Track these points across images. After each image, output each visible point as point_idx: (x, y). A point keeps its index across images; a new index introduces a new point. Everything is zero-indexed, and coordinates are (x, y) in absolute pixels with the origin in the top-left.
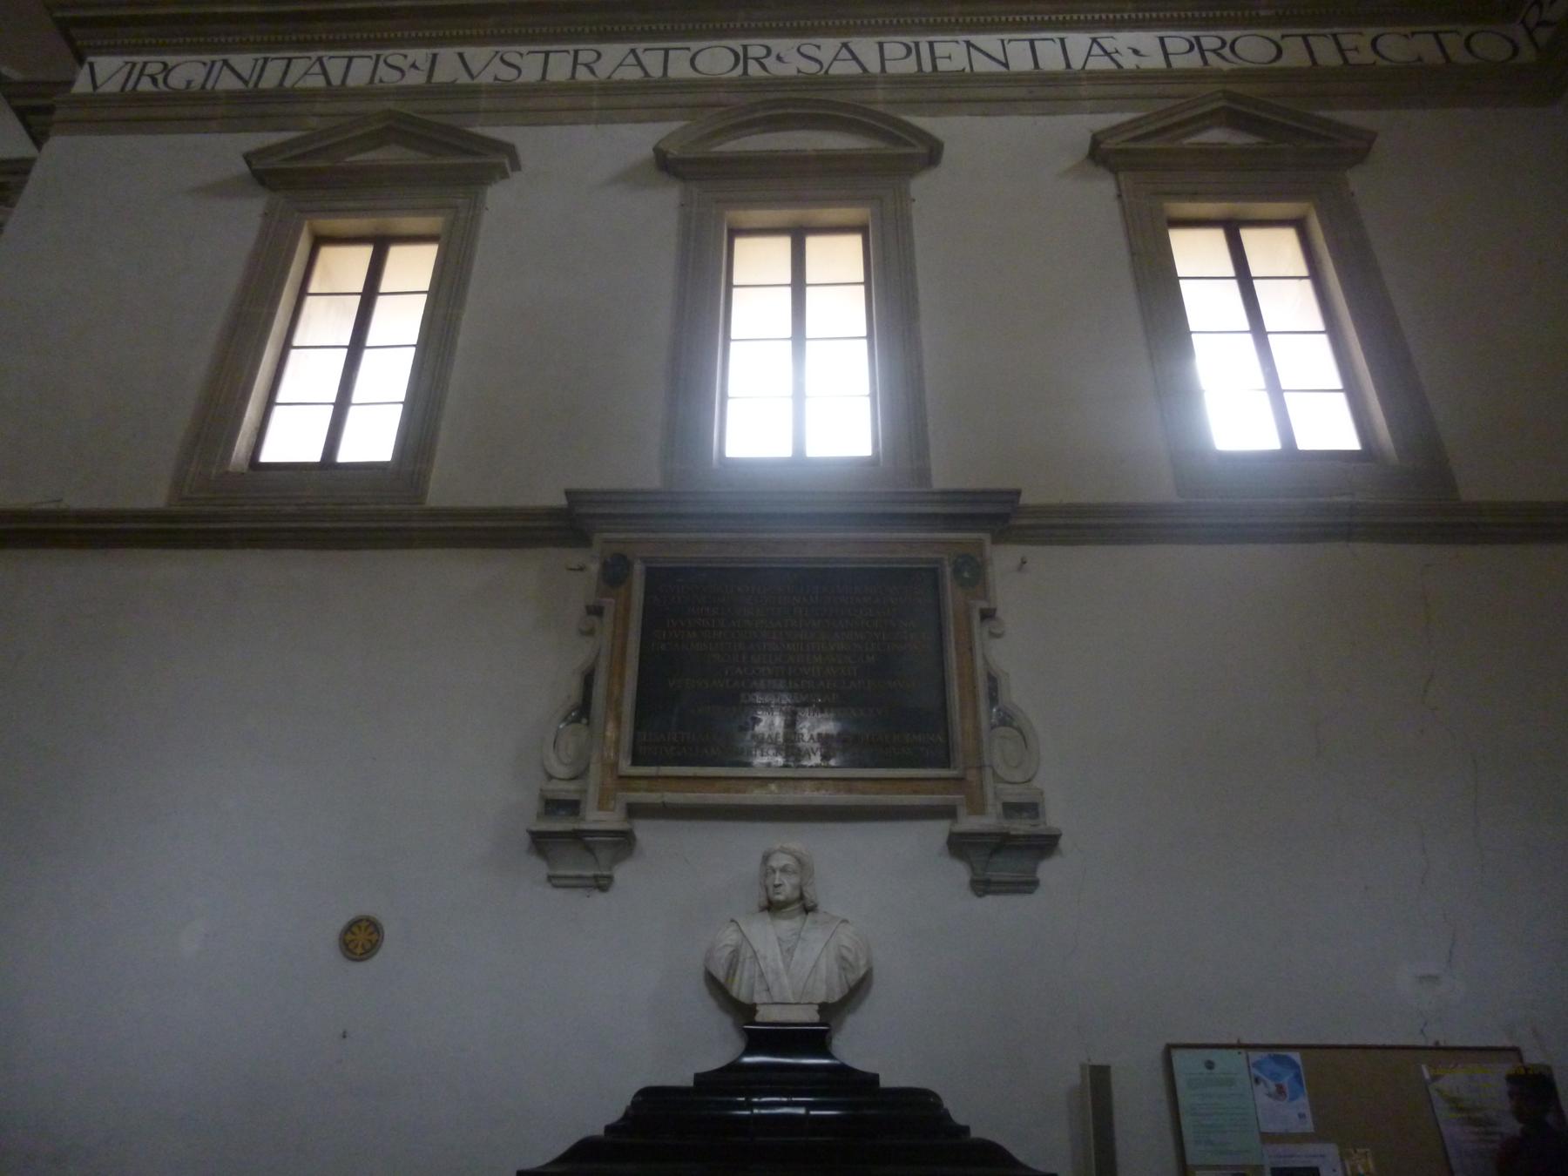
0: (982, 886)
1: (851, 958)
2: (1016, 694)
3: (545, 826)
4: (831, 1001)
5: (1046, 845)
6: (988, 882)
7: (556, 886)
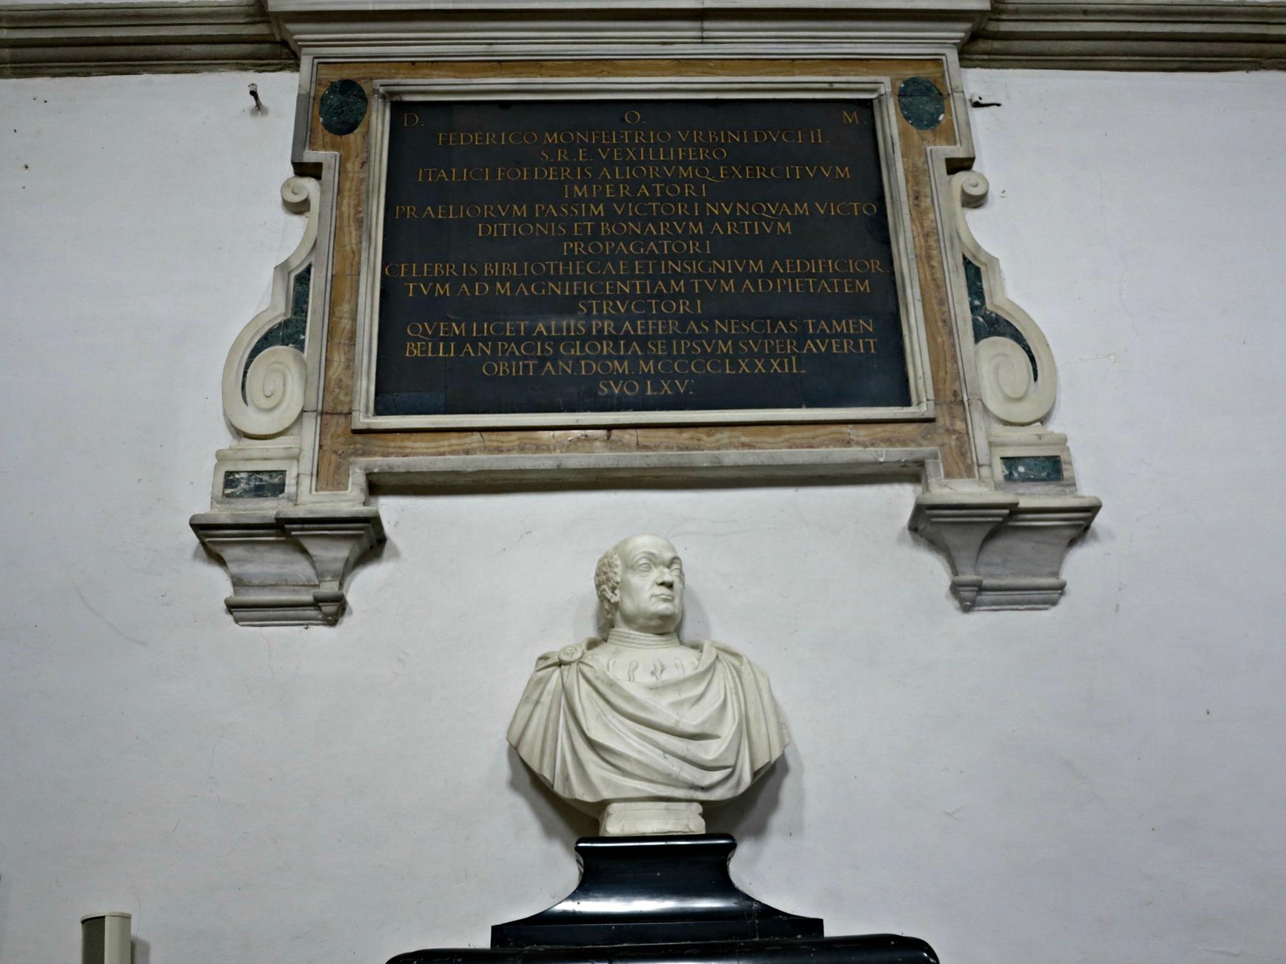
0: (968, 596)
2: (1012, 291)
3: (224, 514)
5: (1080, 523)
6: (981, 588)
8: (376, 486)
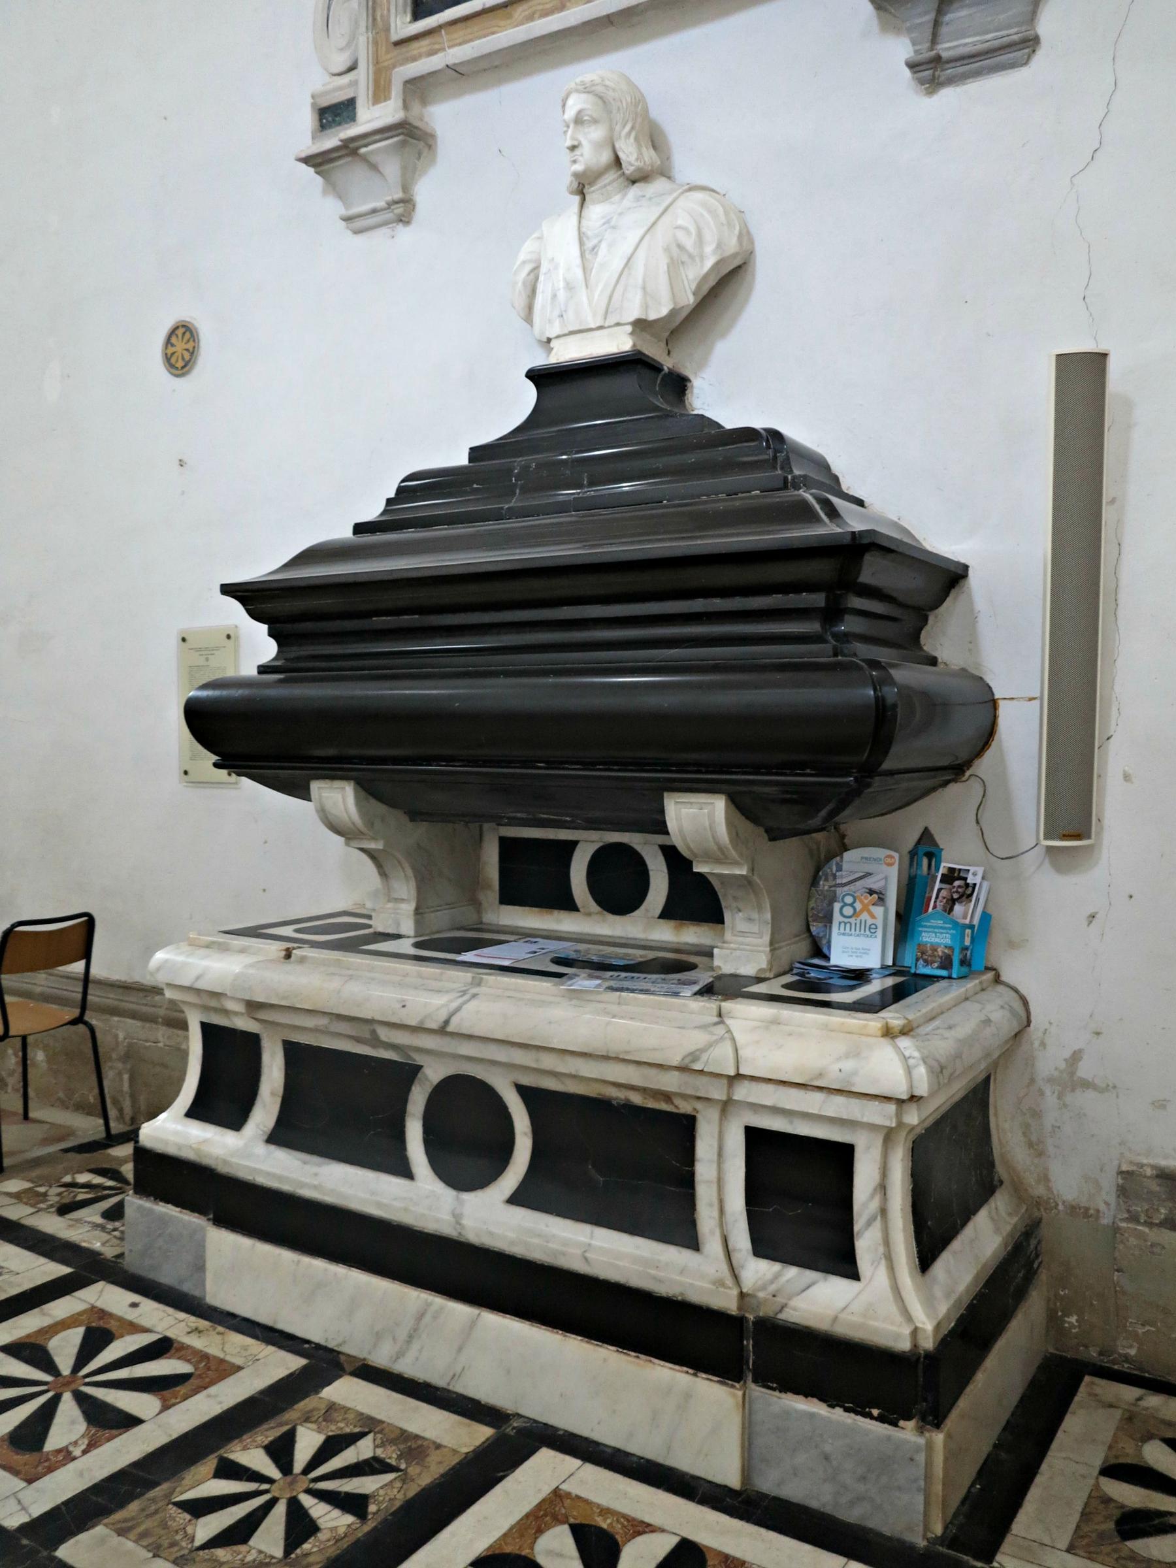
1: (689, 243)
4: (652, 316)
7: (357, 232)
8: (420, 89)
